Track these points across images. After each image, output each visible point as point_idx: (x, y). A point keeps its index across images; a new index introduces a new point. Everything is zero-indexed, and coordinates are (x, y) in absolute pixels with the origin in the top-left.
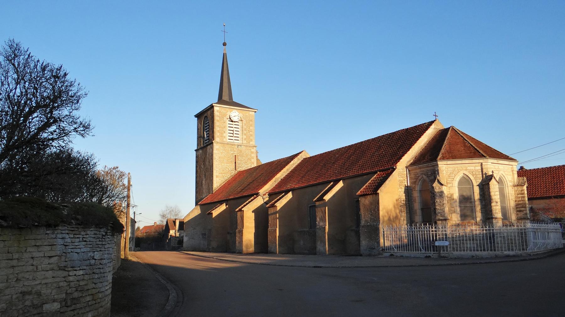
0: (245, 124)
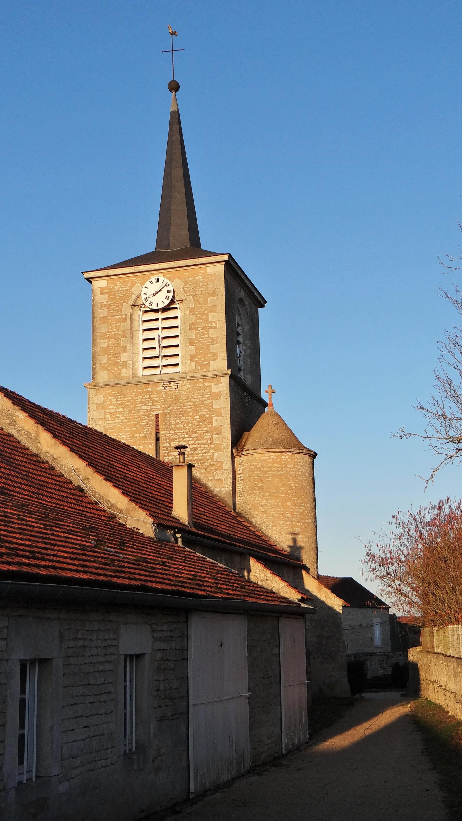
0: (191, 310)
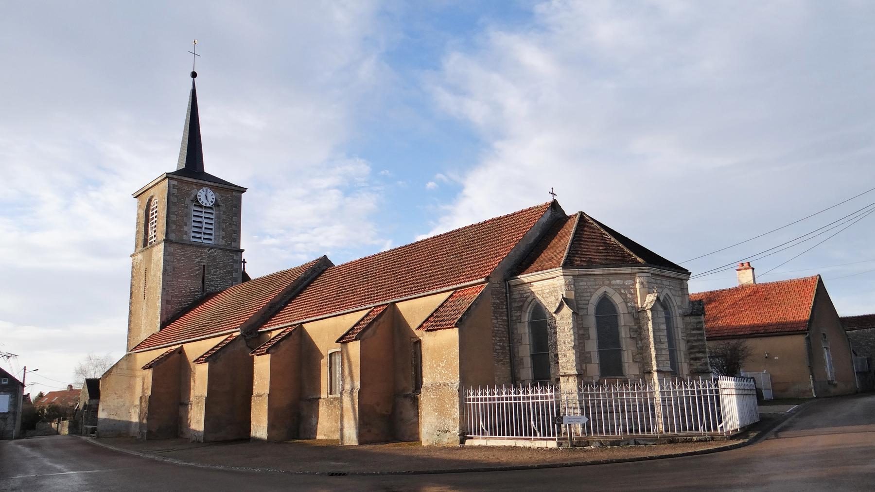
0: (224, 212)
